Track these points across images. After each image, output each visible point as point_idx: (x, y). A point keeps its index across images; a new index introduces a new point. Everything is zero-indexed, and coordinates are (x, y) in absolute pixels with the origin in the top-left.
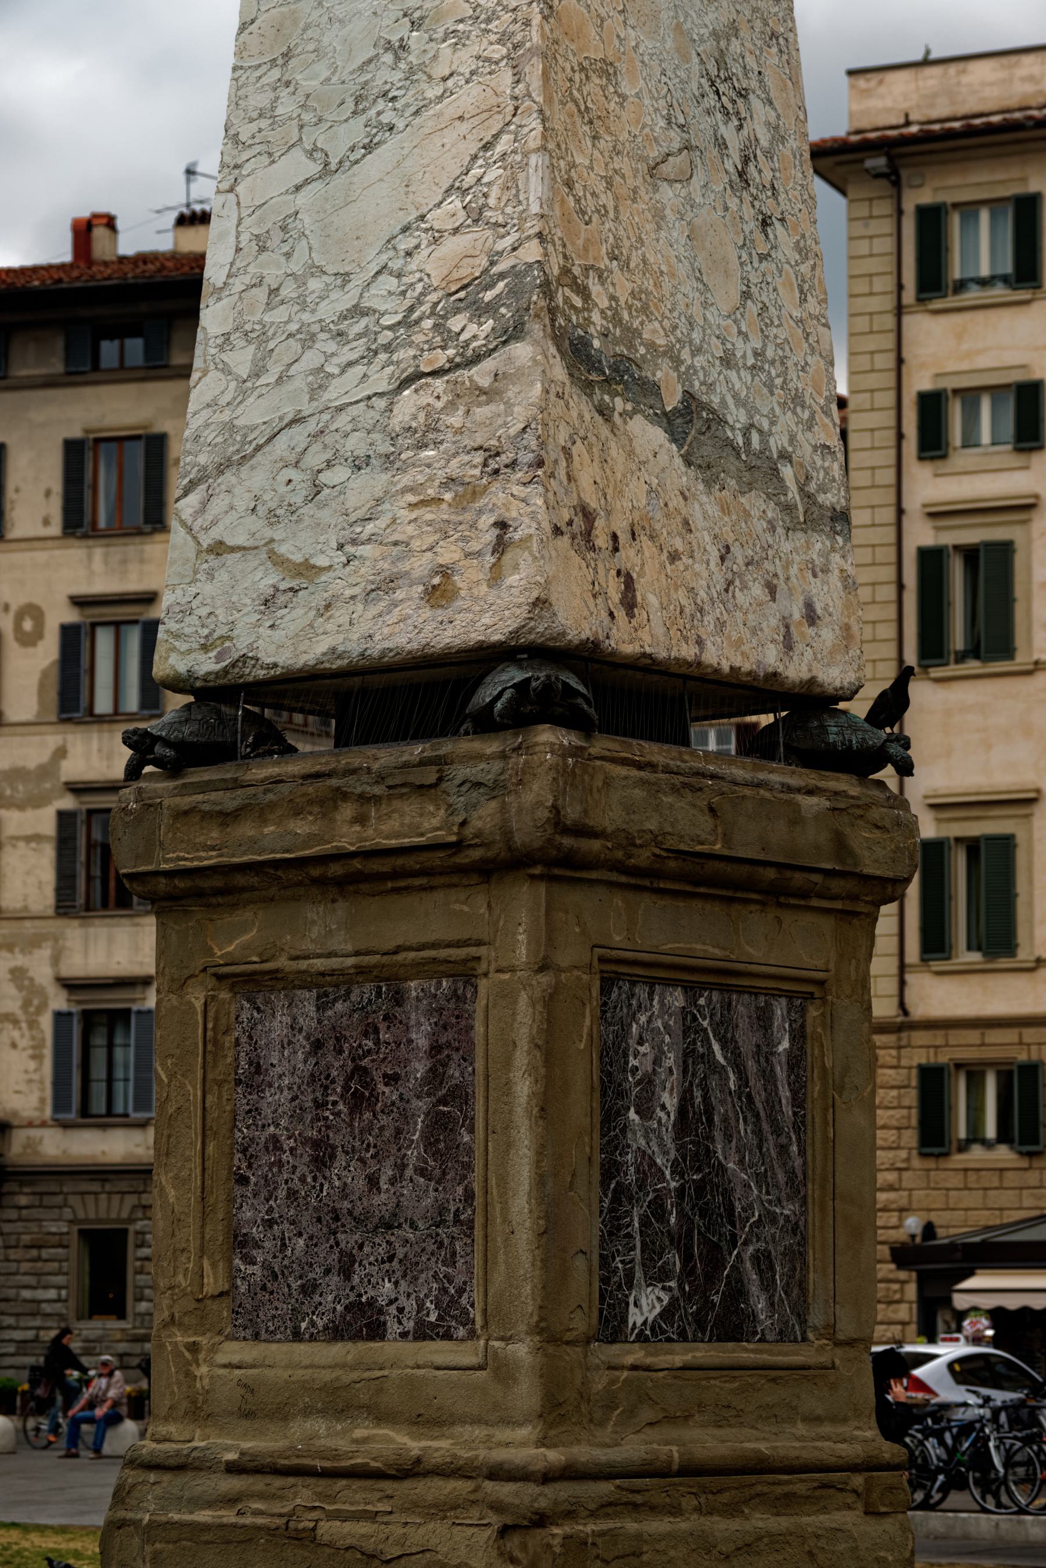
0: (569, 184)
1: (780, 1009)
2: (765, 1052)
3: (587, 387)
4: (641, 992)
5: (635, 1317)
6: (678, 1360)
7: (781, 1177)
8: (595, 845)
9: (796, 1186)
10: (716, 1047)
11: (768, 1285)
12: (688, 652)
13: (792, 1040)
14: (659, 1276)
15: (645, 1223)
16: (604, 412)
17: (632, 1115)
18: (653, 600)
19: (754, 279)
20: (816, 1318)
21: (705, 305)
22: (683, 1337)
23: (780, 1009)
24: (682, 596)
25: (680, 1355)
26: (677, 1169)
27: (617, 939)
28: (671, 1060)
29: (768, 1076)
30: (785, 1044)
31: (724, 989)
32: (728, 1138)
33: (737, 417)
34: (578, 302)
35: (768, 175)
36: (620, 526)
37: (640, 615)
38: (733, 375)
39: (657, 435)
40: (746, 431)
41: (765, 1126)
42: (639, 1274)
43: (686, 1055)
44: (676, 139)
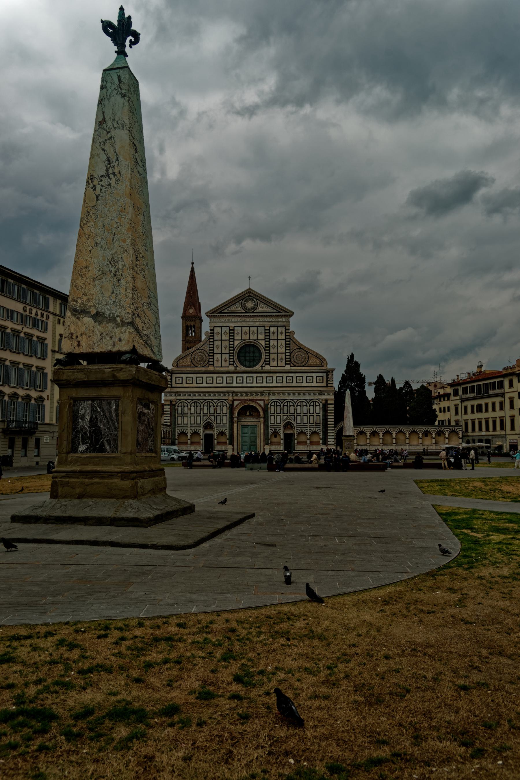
0: (76, 286)
1: (113, 402)
2: (110, 409)
3: (75, 315)
4: (82, 402)
5: (80, 449)
6: (86, 456)
7: (113, 428)
8: (62, 382)
9: (116, 429)
10: (98, 409)
11: (109, 444)
12: (90, 350)
13: (116, 406)
14: (84, 443)
15: (82, 436)
16: (78, 318)
17: (80, 420)
18: (84, 344)
19: (115, 290)
20: (119, 449)
21: (103, 297)
22: (90, 452)
23: (113, 402)
24: (91, 342)
25: (88, 455)
26: (89, 428)
27: (74, 395)
28: (88, 411)
29: (110, 413)
30: (114, 407)
31: (110, 400)
32: (101, 422)
33: (107, 312)
34: (75, 303)
35: (121, 273)
36: (79, 334)
37: (81, 347)
38: (108, 306)
39: (90, 319)
40: (109, 315)
41: (109, 420)
42: (81, 443)
43: (92, 411)
44: (100, 273)
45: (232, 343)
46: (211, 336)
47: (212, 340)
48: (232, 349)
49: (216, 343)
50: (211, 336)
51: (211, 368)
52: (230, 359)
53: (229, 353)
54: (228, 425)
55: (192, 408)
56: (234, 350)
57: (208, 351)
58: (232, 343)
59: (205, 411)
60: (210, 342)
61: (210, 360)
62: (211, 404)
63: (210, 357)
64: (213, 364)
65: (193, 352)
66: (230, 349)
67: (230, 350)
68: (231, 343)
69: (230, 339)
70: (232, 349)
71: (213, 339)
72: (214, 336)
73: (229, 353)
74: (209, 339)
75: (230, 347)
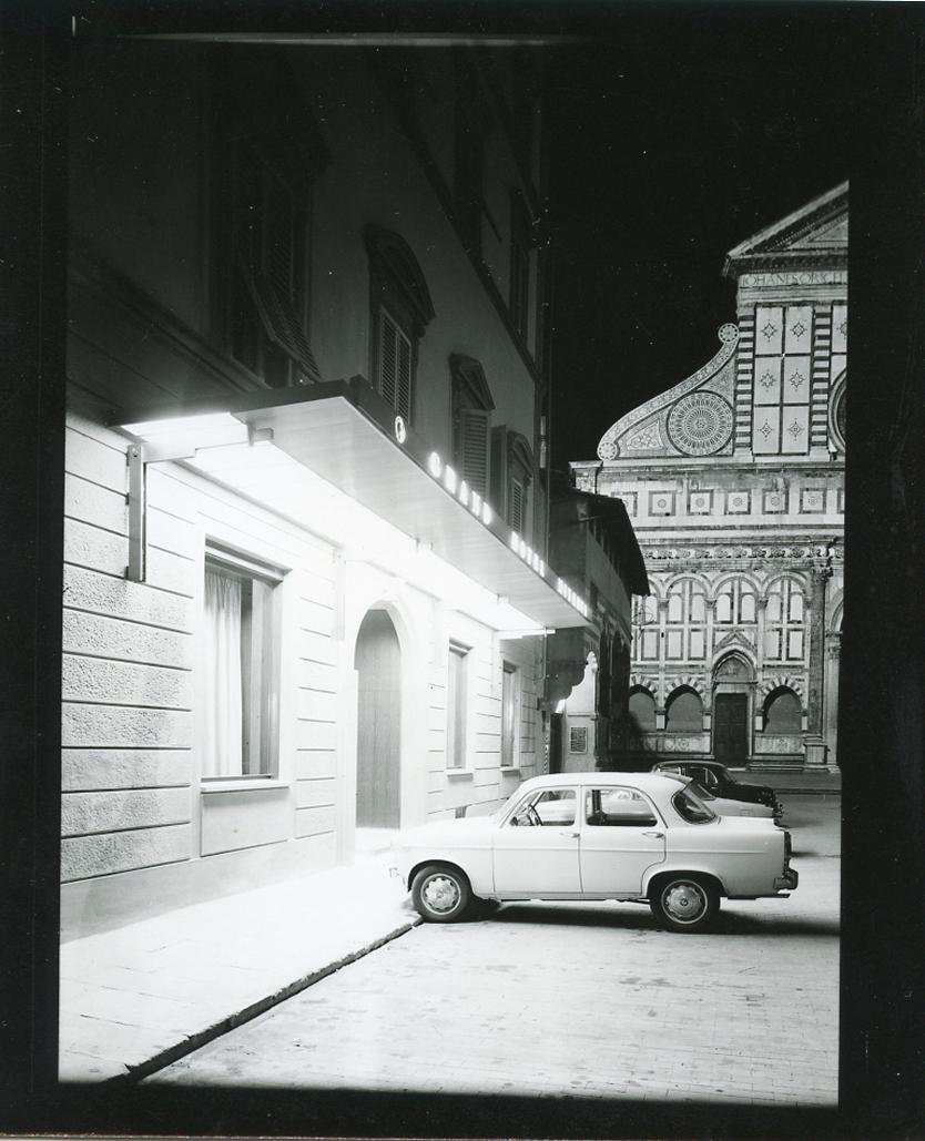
45: (825, 364)
46: (745, 340)
47: (749, 355)
48: (824, 386)
49: (762, 366)
50: (745, 340)
51: (743, 457)
52: (811, 423)
53: (813, 403)
54: (806, 663)
55: (675, 603)
56: (828, 391)
57: (731, 400)
58: (825, 364)
59: (724, 611)
60: (738, 362)
61: (739, 429)
62: (746, 588)
63: (739, 419)
64: (750, 445)
65: (675, 403)
66: (817, 386)
67: (813, 392)
68: (818, 364)
69: (814, 348)
70: (824, 386)
71: (753, 350)
72: (753, 340)
73: (813, 403)
74: (738, 350)
75: (813, 381)
